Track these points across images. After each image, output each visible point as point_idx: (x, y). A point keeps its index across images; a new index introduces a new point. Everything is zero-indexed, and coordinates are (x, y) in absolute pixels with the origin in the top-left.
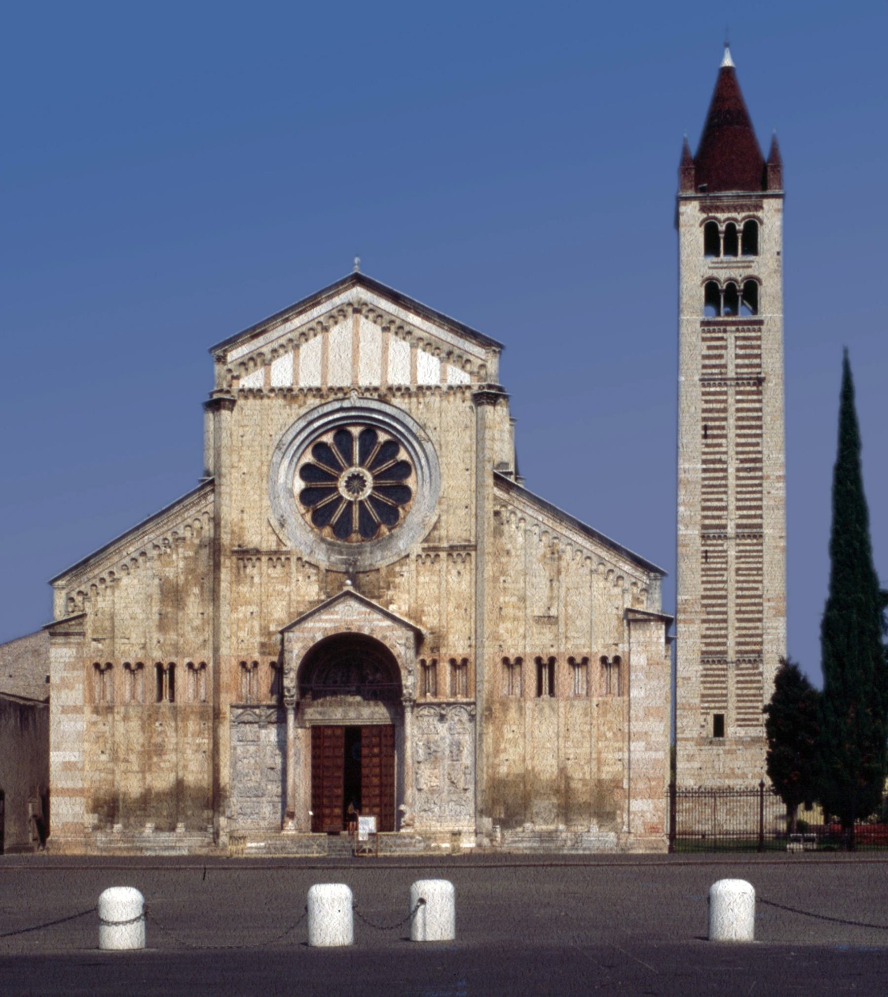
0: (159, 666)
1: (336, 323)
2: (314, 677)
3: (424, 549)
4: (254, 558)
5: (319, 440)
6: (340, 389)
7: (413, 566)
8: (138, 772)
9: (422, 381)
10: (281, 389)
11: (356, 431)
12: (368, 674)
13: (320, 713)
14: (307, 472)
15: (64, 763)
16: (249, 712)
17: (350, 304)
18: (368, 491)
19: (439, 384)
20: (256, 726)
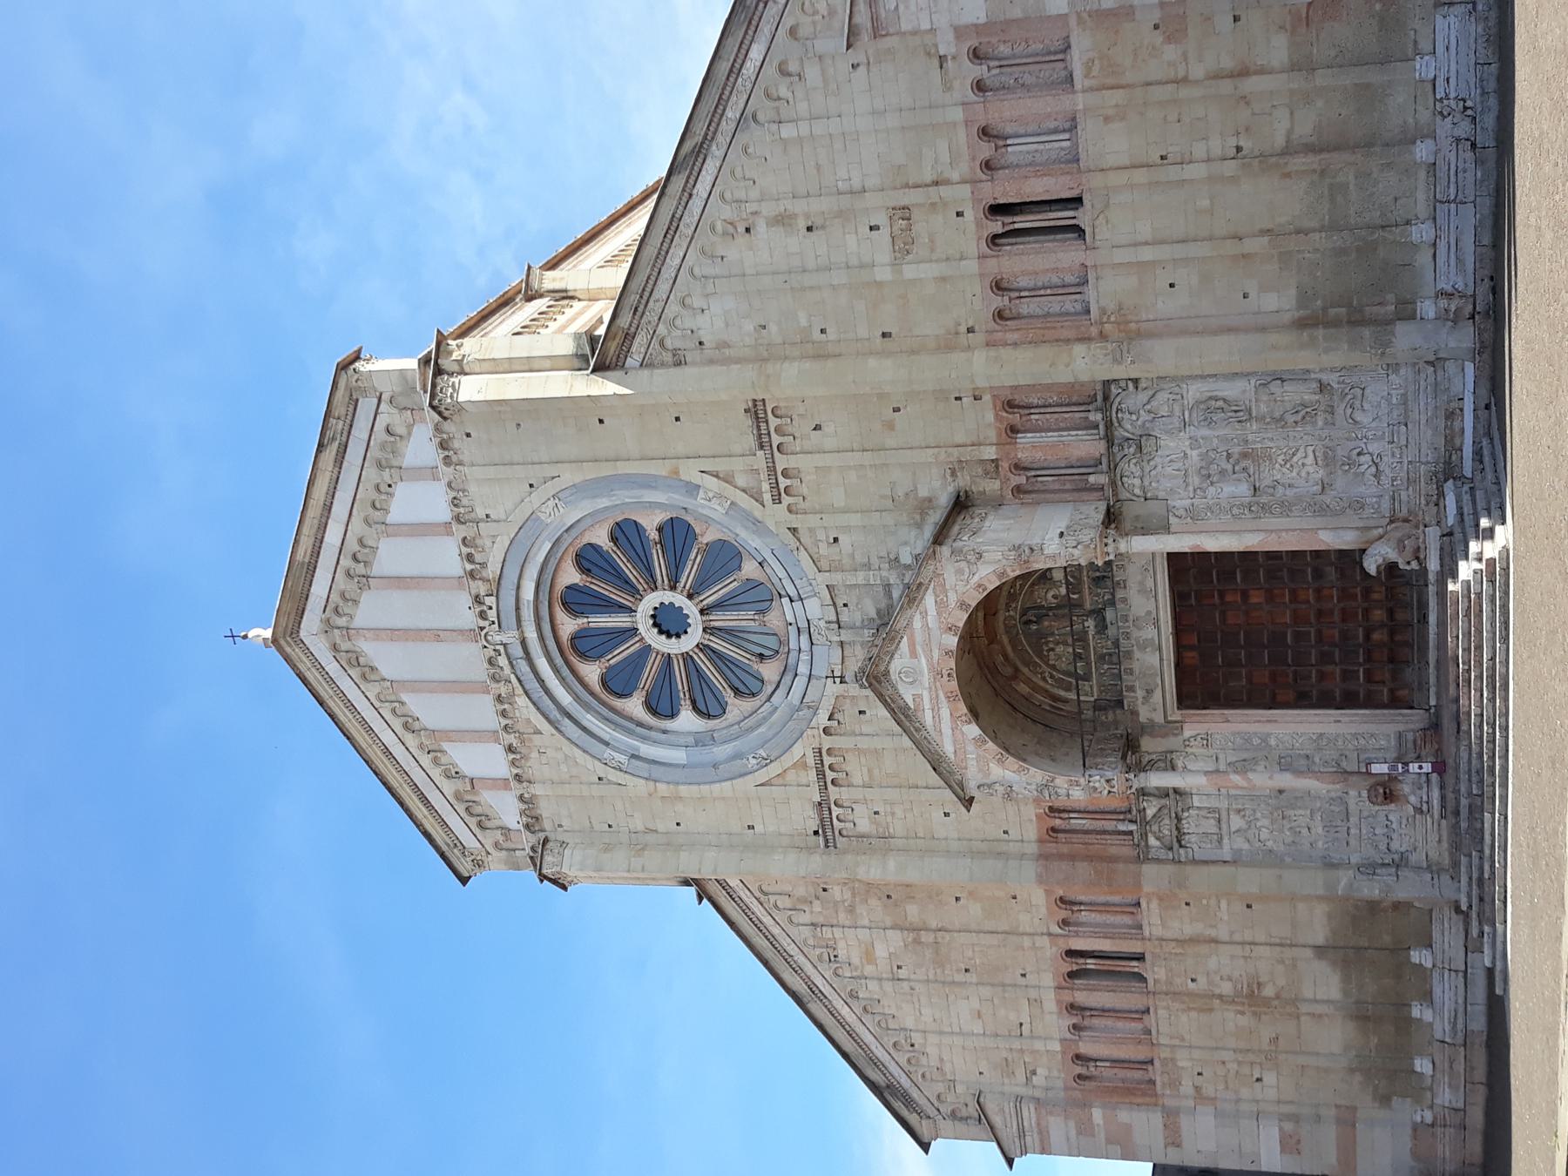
0: (1072, 975)
1: (372, 669)
3: (777, 500)
4: (836, 811)
5: (597, 688)
6: (491, 662)
7: (813, 520)
8: (1299, 1025)
9: (444, 513)
10: (513, 763)
11: (569, 625)
12: (1053, 596)
13: (1149, 692)
14: (660, 705)
15: (1282, 1151)
16: (1155, 828)
17: (335, 648)
18: (679, 599)
19: (444, 482)
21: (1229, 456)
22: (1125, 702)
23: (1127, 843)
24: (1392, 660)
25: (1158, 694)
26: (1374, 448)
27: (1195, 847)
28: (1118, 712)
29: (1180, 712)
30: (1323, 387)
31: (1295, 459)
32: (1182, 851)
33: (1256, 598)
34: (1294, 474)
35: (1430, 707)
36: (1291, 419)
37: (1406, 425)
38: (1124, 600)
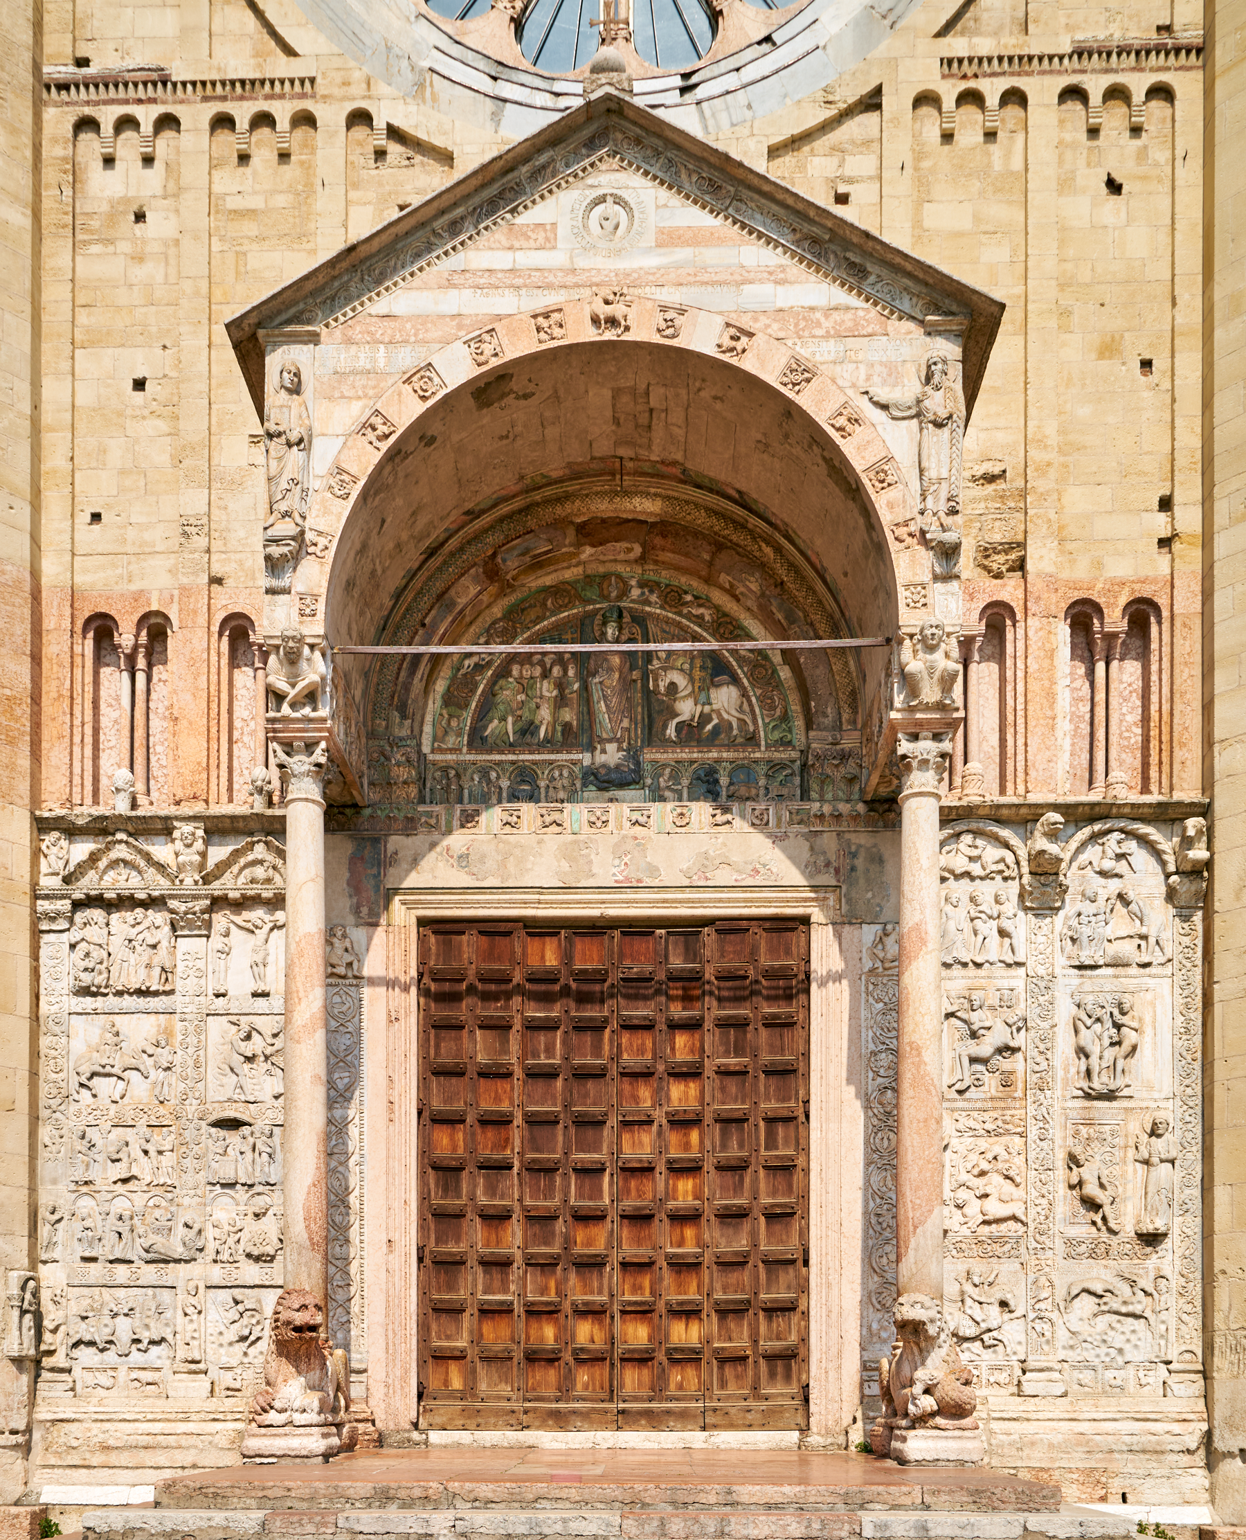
2: (434, 705)
20: (158, 917)
21: (1006, 1050)
22: (437, 808)
23: (77, 789)
24: (533, 1358)
25: (461, 879)
26: (1013, 1332)
27: (74, 936)
28: (413, 791)
29: (414, 921)
30: (1151, 1239)
31: (997, 1179)
32: (65, 905)
33: (681, 1095)
34: (964, 1177)
35: (422, 1432)
36: (1088, 1173)
37: (1065, 1395)
38: (682, 821)
